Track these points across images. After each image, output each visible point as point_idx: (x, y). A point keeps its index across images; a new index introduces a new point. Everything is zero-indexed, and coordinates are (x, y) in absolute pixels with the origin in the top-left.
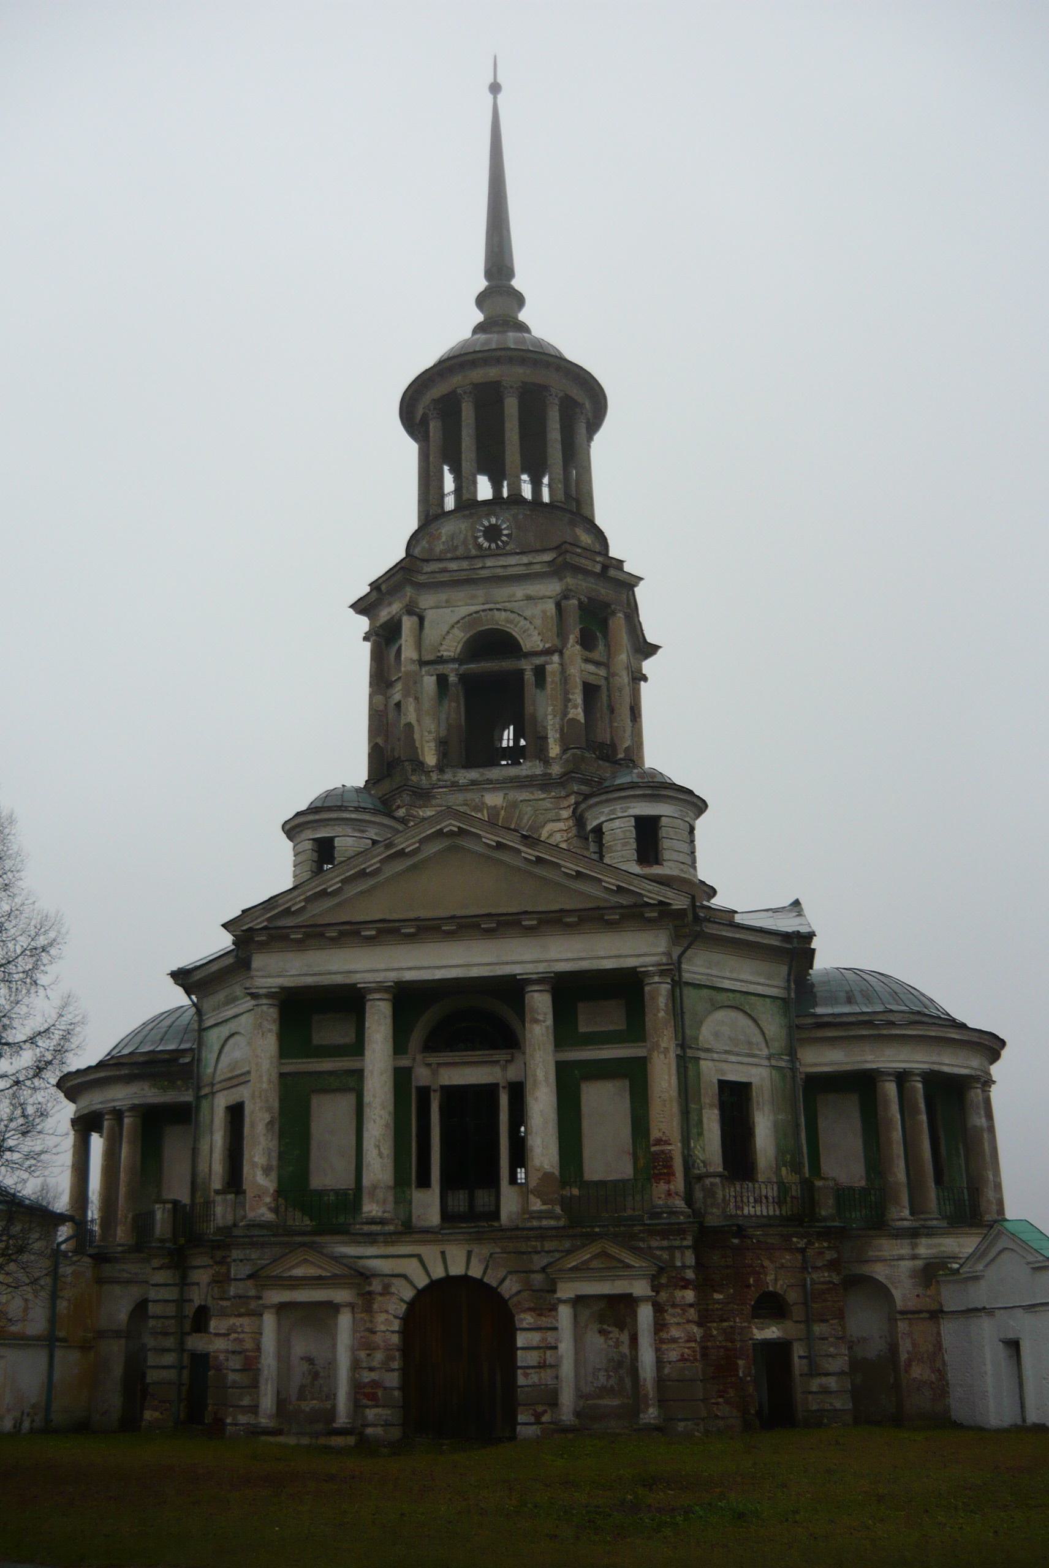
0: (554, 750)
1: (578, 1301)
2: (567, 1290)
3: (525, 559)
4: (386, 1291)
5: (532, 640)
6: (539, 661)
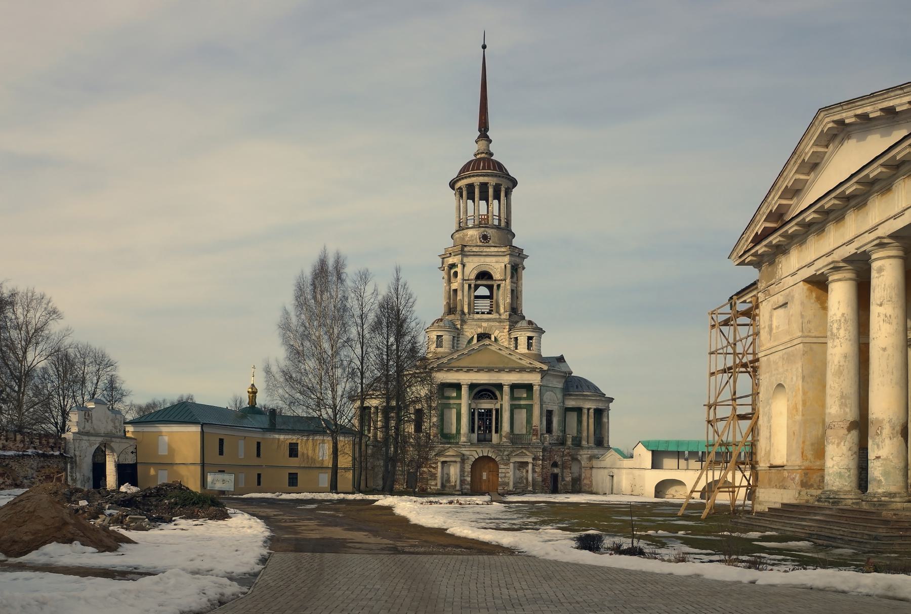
0: (502, 311)
1: (514, 463)
2: (513, 460)
3: (496, 249)
4: (468, 458)
5: (497, 275)
6: (499, 283)
